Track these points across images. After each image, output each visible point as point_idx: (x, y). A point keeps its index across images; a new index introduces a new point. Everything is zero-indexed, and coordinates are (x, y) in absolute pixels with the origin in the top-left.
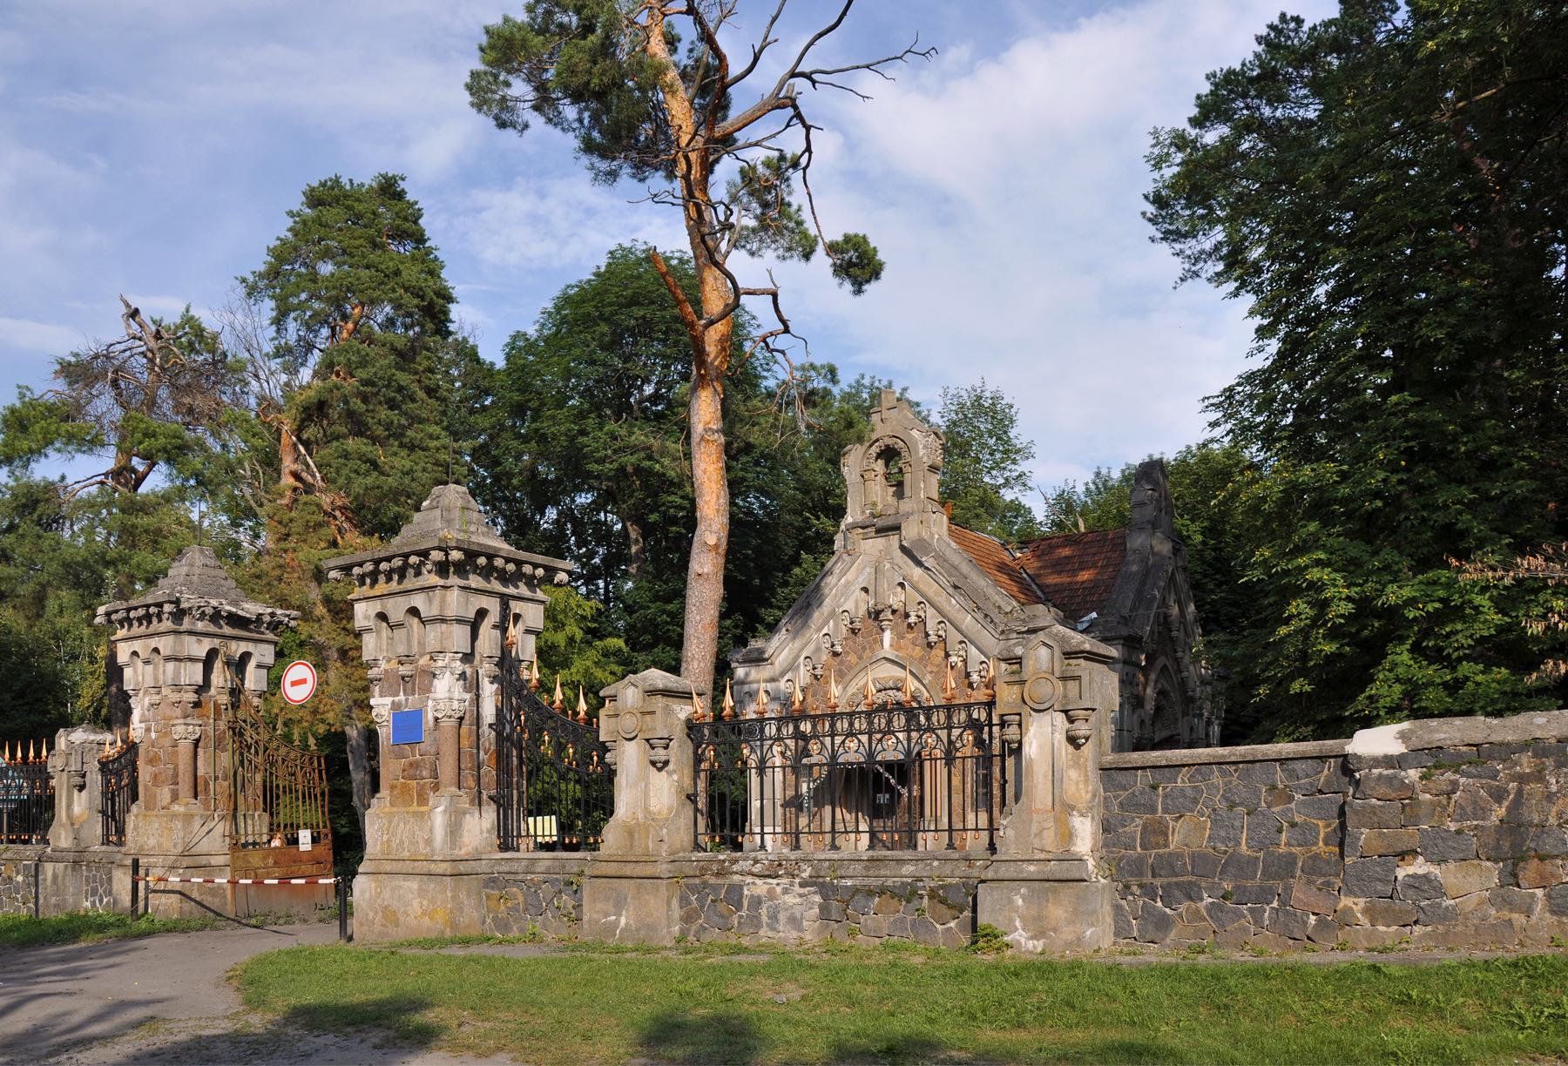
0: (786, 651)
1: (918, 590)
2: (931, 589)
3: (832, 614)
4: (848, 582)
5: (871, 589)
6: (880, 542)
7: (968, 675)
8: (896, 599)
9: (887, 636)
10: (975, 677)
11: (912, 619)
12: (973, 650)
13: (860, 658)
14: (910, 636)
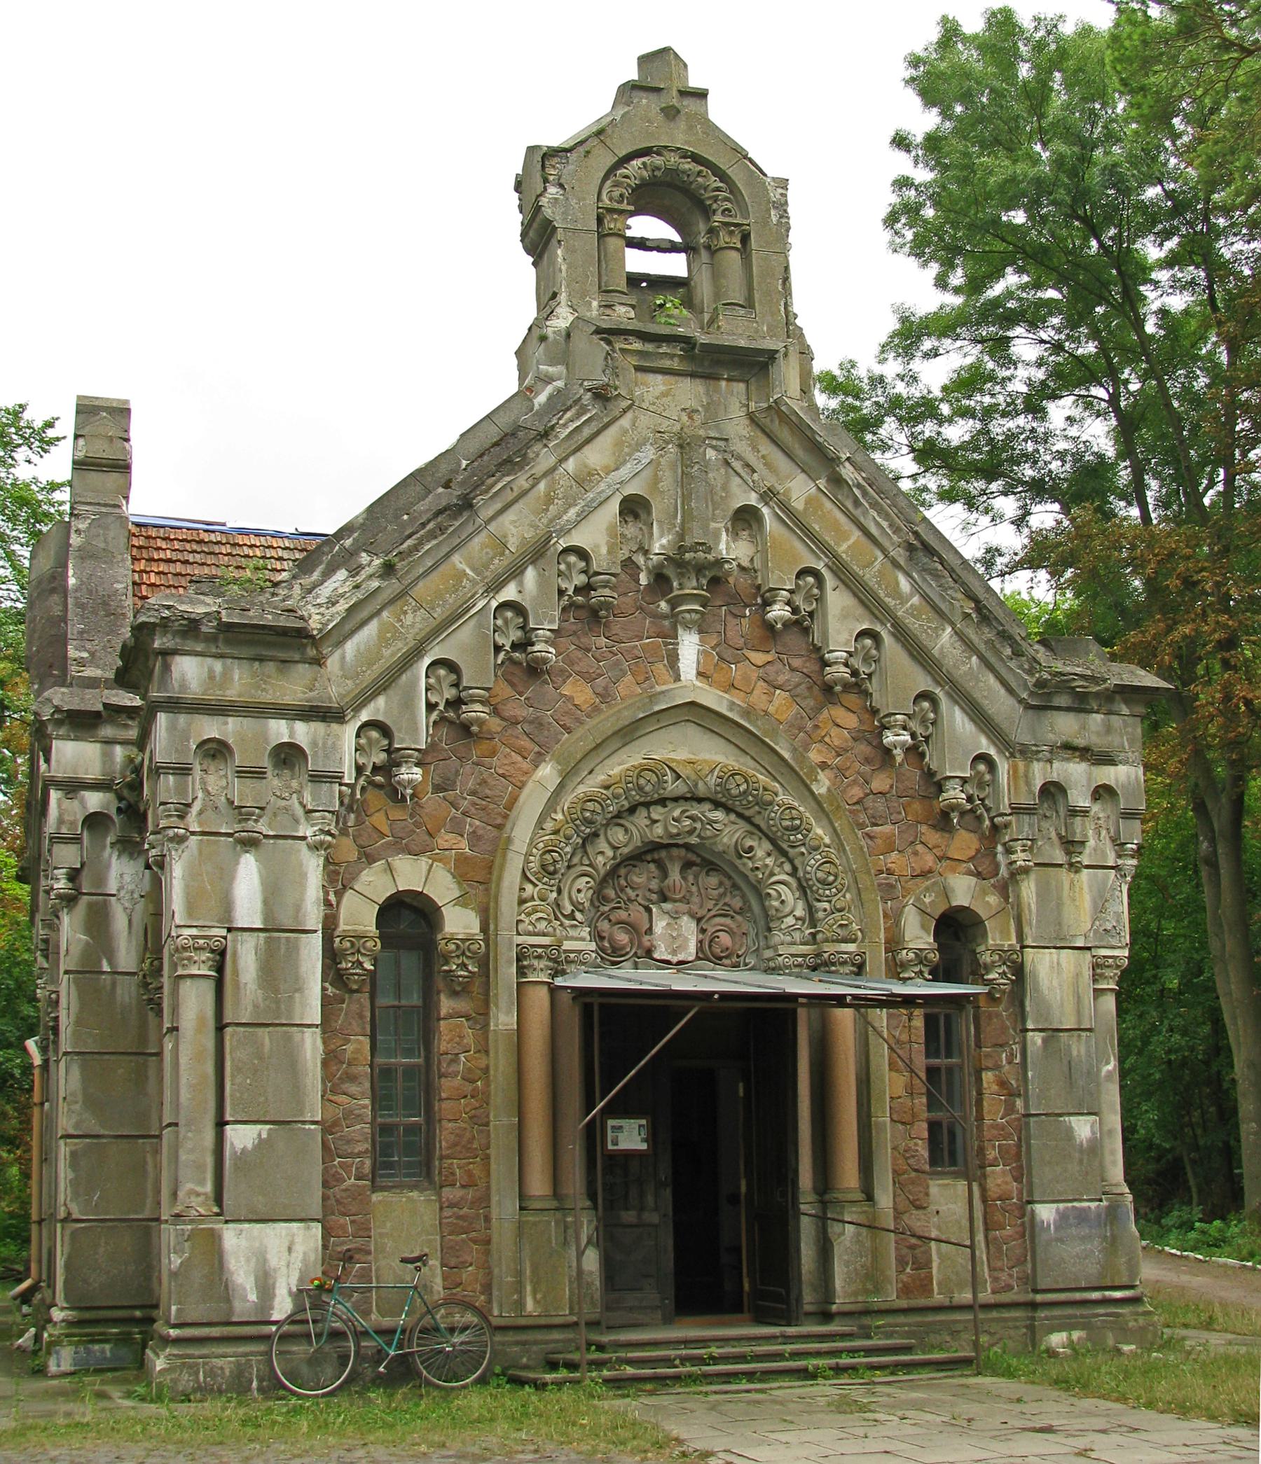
0: (370, 631)
1: (808, 534)
3: (537, 553)
7: (935, 784)
8: (733, 549)
9: (689, 647)
10: (954, 794)
12: (958, 720)
13: (605, 696)
14: (759, 658)
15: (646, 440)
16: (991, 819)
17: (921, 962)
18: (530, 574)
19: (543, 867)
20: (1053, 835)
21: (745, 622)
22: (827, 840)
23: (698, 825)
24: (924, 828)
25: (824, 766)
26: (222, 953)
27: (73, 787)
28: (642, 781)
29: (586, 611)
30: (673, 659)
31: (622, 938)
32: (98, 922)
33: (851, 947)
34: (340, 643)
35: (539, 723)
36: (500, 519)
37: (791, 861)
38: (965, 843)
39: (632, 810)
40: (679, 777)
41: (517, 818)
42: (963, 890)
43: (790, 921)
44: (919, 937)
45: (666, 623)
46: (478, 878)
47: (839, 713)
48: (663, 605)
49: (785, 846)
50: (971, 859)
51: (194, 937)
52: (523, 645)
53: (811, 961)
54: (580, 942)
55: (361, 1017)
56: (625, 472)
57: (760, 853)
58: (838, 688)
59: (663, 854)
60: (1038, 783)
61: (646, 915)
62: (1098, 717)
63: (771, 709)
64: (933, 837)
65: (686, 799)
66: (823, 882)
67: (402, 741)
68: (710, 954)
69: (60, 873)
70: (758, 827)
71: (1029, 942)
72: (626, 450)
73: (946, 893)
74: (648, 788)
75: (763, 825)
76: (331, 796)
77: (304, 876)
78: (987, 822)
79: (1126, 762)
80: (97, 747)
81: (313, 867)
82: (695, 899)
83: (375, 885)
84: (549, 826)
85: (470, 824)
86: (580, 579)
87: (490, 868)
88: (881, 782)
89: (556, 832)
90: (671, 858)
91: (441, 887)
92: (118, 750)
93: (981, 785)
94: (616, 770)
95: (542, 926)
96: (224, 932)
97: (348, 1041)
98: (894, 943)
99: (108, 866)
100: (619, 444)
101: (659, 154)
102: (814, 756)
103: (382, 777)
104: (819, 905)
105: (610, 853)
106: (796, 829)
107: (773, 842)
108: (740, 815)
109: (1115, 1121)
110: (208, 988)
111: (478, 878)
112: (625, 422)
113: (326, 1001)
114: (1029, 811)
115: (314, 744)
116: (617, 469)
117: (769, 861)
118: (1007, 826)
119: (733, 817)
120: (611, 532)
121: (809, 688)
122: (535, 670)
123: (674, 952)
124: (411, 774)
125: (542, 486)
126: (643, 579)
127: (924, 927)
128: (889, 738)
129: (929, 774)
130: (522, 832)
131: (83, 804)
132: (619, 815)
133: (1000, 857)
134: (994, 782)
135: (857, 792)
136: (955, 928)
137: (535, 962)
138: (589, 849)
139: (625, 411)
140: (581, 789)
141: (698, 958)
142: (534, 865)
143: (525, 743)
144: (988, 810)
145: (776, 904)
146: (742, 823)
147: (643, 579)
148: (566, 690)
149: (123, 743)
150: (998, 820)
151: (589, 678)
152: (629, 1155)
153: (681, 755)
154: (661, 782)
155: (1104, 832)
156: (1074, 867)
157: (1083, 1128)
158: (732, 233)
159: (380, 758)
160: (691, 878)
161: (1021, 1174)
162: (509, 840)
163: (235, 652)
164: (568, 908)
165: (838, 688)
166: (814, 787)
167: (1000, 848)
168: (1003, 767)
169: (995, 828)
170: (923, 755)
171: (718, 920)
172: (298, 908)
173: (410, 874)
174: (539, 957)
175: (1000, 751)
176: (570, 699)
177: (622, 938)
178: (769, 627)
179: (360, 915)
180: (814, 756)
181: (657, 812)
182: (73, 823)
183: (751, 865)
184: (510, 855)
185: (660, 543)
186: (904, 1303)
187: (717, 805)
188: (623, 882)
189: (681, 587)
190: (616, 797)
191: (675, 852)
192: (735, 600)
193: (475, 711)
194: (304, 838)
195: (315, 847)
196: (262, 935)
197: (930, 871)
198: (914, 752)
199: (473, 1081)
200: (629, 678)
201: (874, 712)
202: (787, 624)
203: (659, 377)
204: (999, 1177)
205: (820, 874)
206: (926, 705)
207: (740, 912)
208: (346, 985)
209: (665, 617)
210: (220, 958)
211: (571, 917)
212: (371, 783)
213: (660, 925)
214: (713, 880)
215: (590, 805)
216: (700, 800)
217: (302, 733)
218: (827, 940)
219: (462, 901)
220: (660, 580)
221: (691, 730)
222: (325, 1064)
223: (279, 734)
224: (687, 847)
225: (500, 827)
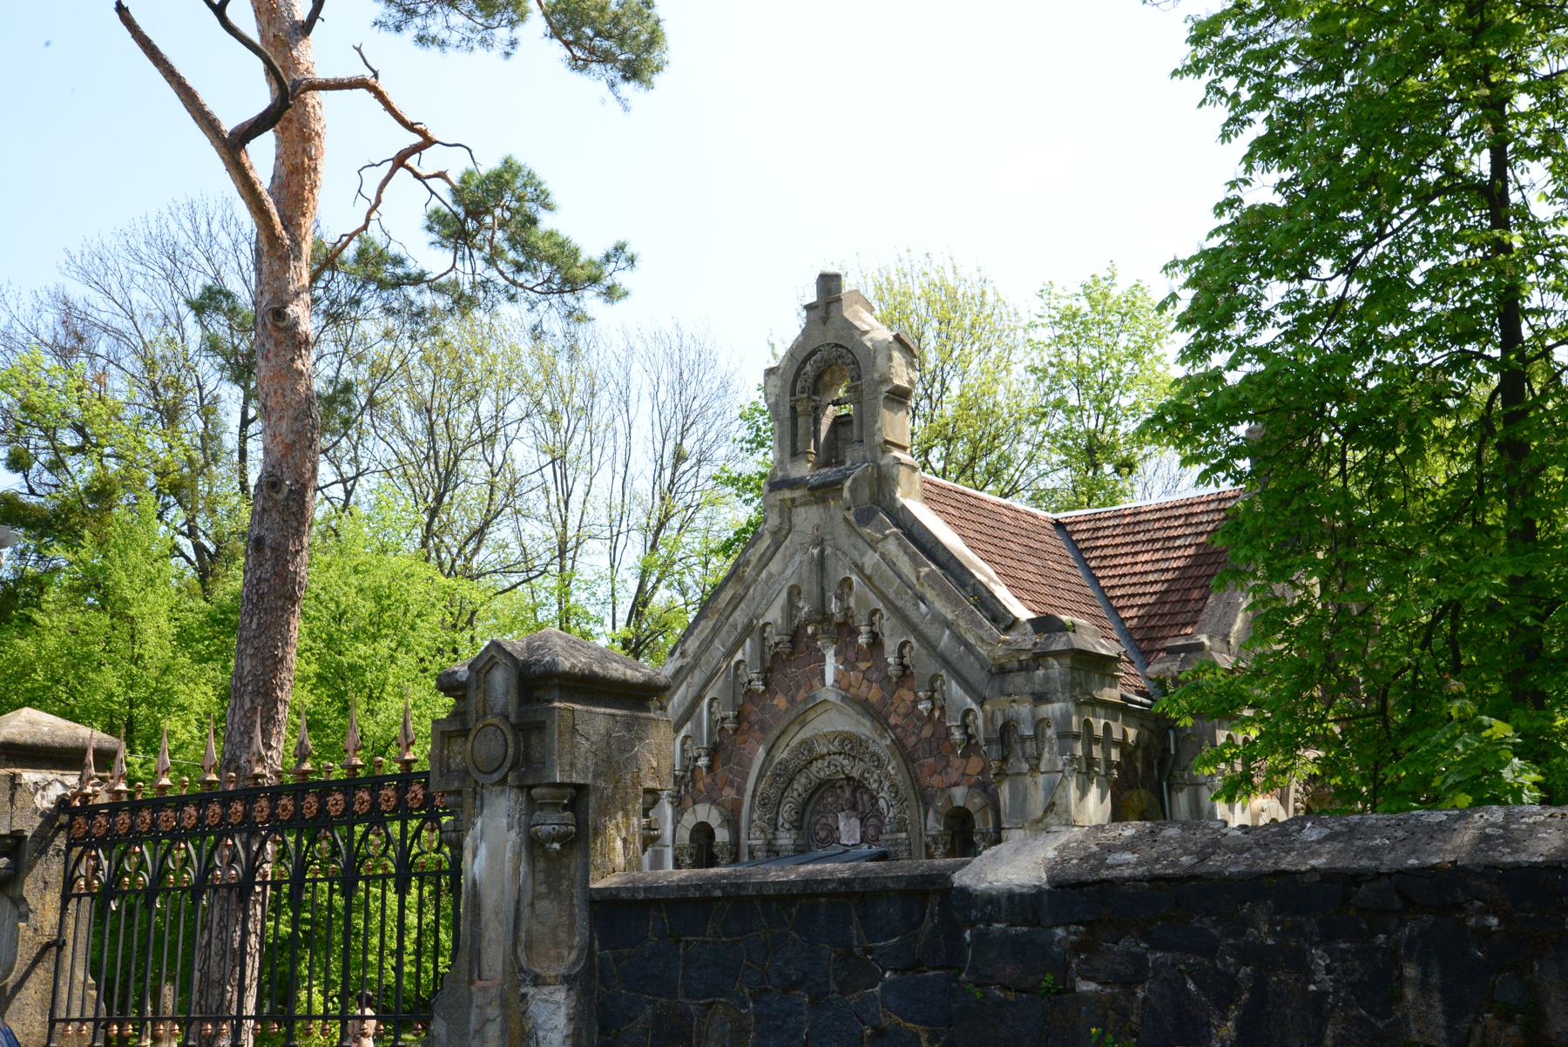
3: (749, 629)
4: (770, 575)
5: (804, 588)
9: (831, 667)
11: (863, 640)
12: (955, 689)
13: (792, 701)
14: (863, 666)
18: (748, 642)
30: (823, 673)
33: (904, 835)
56: (788, 572)
71: (1005, 825)
73: (950, 799)
83: (689, 820)
112: (787, 542)
127: (938, 821)
130: (750, 786)
135: (913, 739)
141: (862, 841)
143: (758, 734)
164: (781, 820)
173: (705, 813)
179: (685, 836)
180: (892, 721)
213: (841, 825)
219: (721, 825)
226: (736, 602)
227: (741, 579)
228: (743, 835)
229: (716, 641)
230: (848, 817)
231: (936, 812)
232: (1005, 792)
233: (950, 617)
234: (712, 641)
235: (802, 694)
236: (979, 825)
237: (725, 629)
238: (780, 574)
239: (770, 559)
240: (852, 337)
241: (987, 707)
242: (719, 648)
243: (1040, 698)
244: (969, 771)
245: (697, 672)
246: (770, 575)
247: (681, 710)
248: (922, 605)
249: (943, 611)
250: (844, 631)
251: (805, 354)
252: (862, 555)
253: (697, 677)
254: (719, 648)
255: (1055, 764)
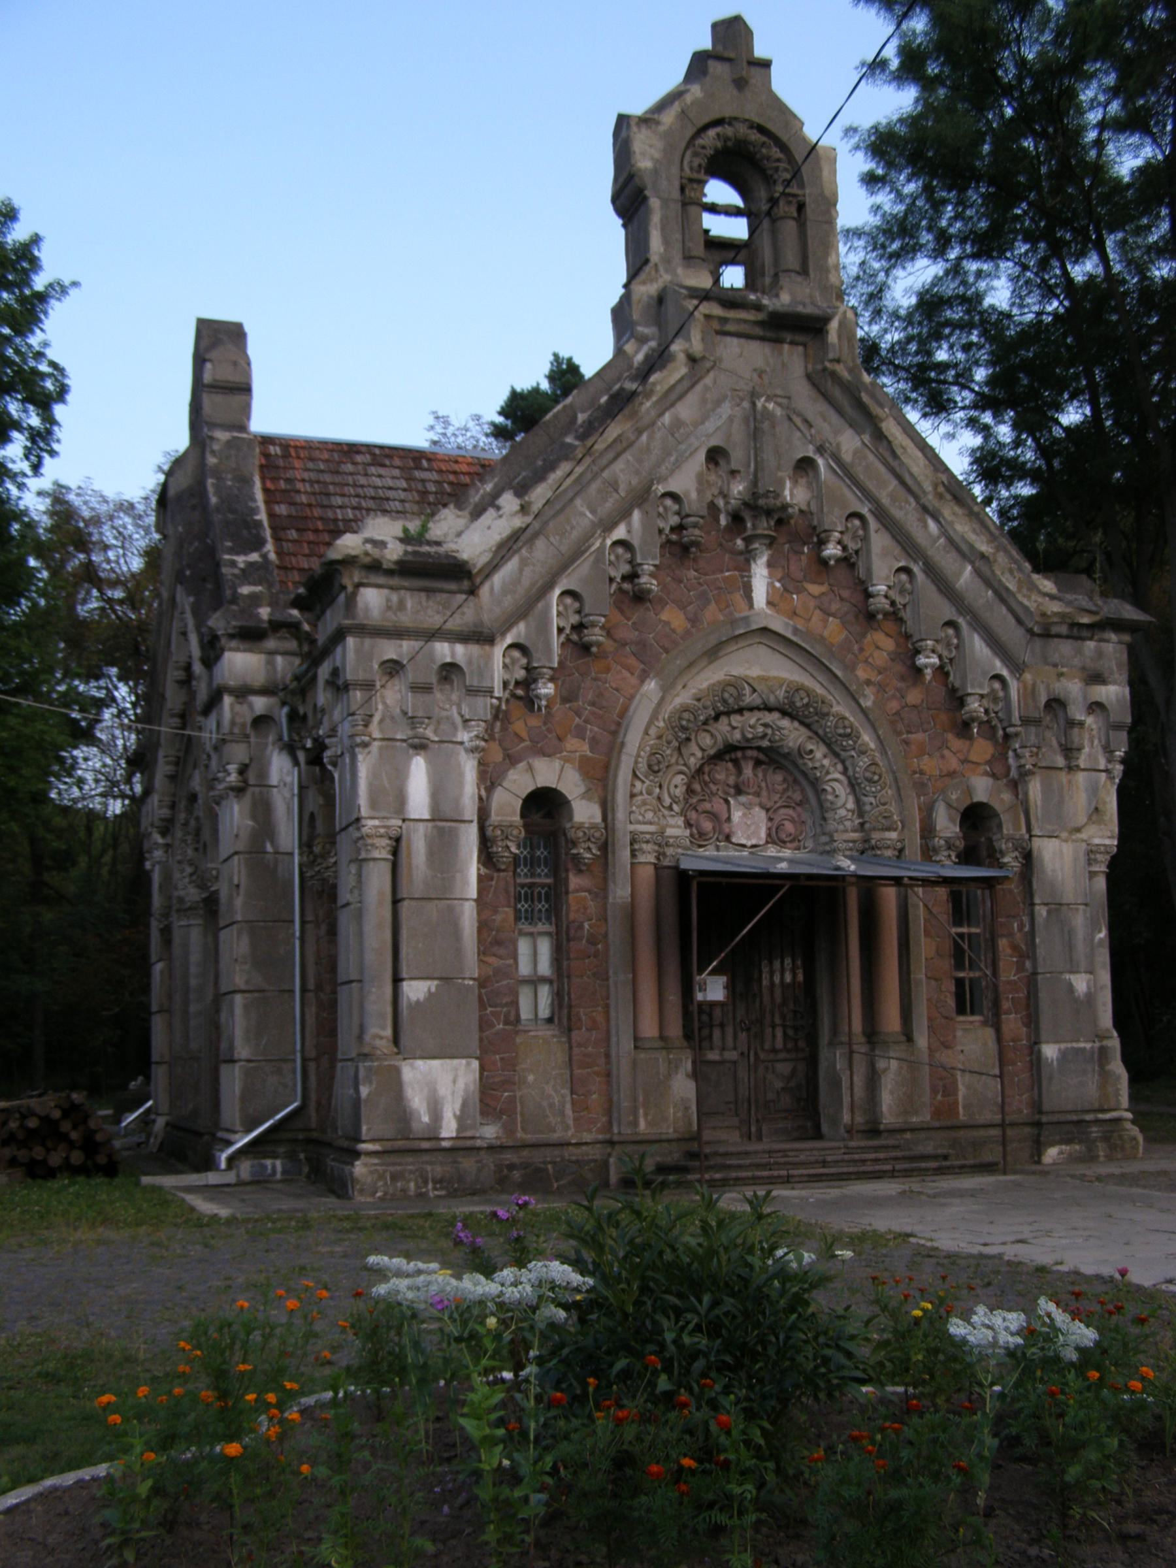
0: (511, 567)
2: (887, 491)
3: (641, 497)
4: (678, 423)
5: (737, 457)
6: (757, 354)
7: (957, 699)
10: (974, 706)
11: (832, 550)
12: (978, 646)
13: (694, 621)
14: (815, 589)
15: (725, 398)
16: (1004, 729)
17: (949, 848)
18: (636, 515)
19: (650, 766)
20: (1055, 743)
21: (803, 558)
22: (872, 745)
23: (769, 731)
24: (950, 736)
25: (868, 682)
26: (398, 840)
27: (243, 692)
28: (726, 695)
29: (680, 548)
30: (748, 590)
31: (707, 826)
32: (263, 811)
33: (894, 835)
34: (488, 576)
35: (642, 645)
36: (613, 467)
37: (843, 762)
38: (982, 749)
39: (717, 718)
40: (755, 691)
41: (628, 726)
42: (982, 788)
43: (842, 812)
44: (947, 826)
45: (742, 558)
46: (600, 776)
47: (880, 638)
48: (739, 542)
49: (837, 749)
50: (988, 763)
51: (376, 827)
52: (632, 577)
53: (860, 846)
54: (676, 829)
55: (507, 892)
56: (710, 426)
57: (818, 755)
58: (880, 617)
59: (739, 754)
60: (1043, 699)
61: (725, 807)
62: (1091, 644)
63: (826, 634)
64: (956, 743)
65: (759, 709)
66: (870, 781)
67: (539, 660)
68: (774, 838)
69: (232, 768)
70: (816, 733)
72: (709, 406)
73: (969, 791)
74: (731, 701)
75: (821, 732)
76: (483, 707)
77: (461, 775)
78: (1001, 733)
79: (1114, 683)
80: (263, 656)
81: (469, 769)
82: (764, 793)
83: (520, 782)
84: (653, 731)
85: (592, 729)
86: (674, 520)
87: (607, 767)
88: (914, 696)
89: (659, 737)
90: (745, 758)
91: (571, 784)
92: (279, 659)
93: (995, 700)
94: (705, 685)
95: (649, 815)
96: (400, 823)
97: (496, 912)
98: (928, 830)
99: (269, 763)
100: (704, 401)
101: (730, 124)
102: (862, 673)
103: (523, 691)
104: (865, 799)
105: (699, 754)
106: (848, 736)
107: (828, 745)
108: (802, 723)
109: (1105, 977)
110: (386, 868)
111: (600, 776)
112: (708, 380)
113: (480, 878)
114: (1037, 722)
115: (470, 663)
116: (703, 423)
117: (826, 762)
118: (1017, 735)
119: (796, 724)
120: (701, 481)
121: (856, 617)
122: (640, 597)
123: (749, 838)
124: (546, 689)
125: (644, 437)
126: (723, 521)
127: (951, 819)
128: (922, 660)
129: (953, 691)
130: (633, 739)
131: (251, 706)
132: (705, 723)
133: (1011, 761)
134: (1007, 698)
135: (894, 705)
136: (975, 817)
137: (644, 846)
138: (684, 750)
139: (708, 371)
140: (678, 701)
142: (643, 767)
143: (632, 661)
144: (1001, 721)
145: (830, 797)
146: (803, 730)
147: (723, 521)
148: (664, 617)
149: (285, 653)
150: (1011, 730)
151: (682, 607)
152: (713, 1004)
153: (754, 672)
154: (740, 696)
155: (1096, 742)
156: (1071, 769)
157: (1081, 984)
158: (790, 203)
159: (520, 674)
160: (760, 775)
161: (1032, 1020)
162: (623, 744)
163: (406, 584)
164: (667, 801)
165: (880, 617)
166: (861, 701)
167: (1011, 754)
168: (1014, 686)
169: (1007, 736)
170: (947, 674)
171: (783, 811)
172: (457, 801)
173: (545, 773)
174: (647, 842)
175: (1011, 672)
176: (667, 623)
177: (707, 826)
178: (824, 562)
180: (862, 673)
181: (736, 720)
182: (243, 725)
183: (810, 765)
184: (624, 758)
185: (738, 488)
186: (936, 1124)
187: (784, 713)
188: (707, 778)
189: (754, 527)
190: (705, 708)
191: (749, 753)
192: (797, 539)
193: (595, 635)
194: (462, 743)
195: (473, 750)
196: (430, 825)
197: (954, 772)
198: (941, 671)
199: (595, 944)
200: (713, 606)
201: (908, 637)
202: (839, 560)
203: (735, 341)
204: (1013, 1023)
205: (868, 775)
206: (951, 631)
207: (800, 804)
208: (494, 865)
209: (741, 553)
210: (397, 844)
211: (670, 808)
212: (513, 695)
213: (737, 815)
214: (779, 777)
215: (686, 715)
216: (770, 709)
217: (459, 652)
218: (874, 829)
220: (736, 519)
221: (763, 651)
222: (480, 931)
223: (444, 656)
224: (759, 749)
225: (614, 733)
226: (620, 447)
227: (634, 414)
228: (620, 815)
229: (578, 502)
230: (748, 807)
231: (949, 806)
232: (1035, 788)
233: (984, 548)
234: (572, 500)
235: (712, 612)
236: (1008, 829)
237: (594, 487)
238: (696, 425)
239: (681, 397)
240: (787, 125)
241: (1028, 676)
242: (583, 515)
243: (1096, 678)
244: (973, 757)
245: (540, 543)
246: (678, 423)
247: (509, 601)
248: (932, 525)
249: (972, 537)
250: (791, 534)
251: (706, 119)
252: (837, 432)
253: (542, 552)
254: (583, 515)
255: (1096, 760)
